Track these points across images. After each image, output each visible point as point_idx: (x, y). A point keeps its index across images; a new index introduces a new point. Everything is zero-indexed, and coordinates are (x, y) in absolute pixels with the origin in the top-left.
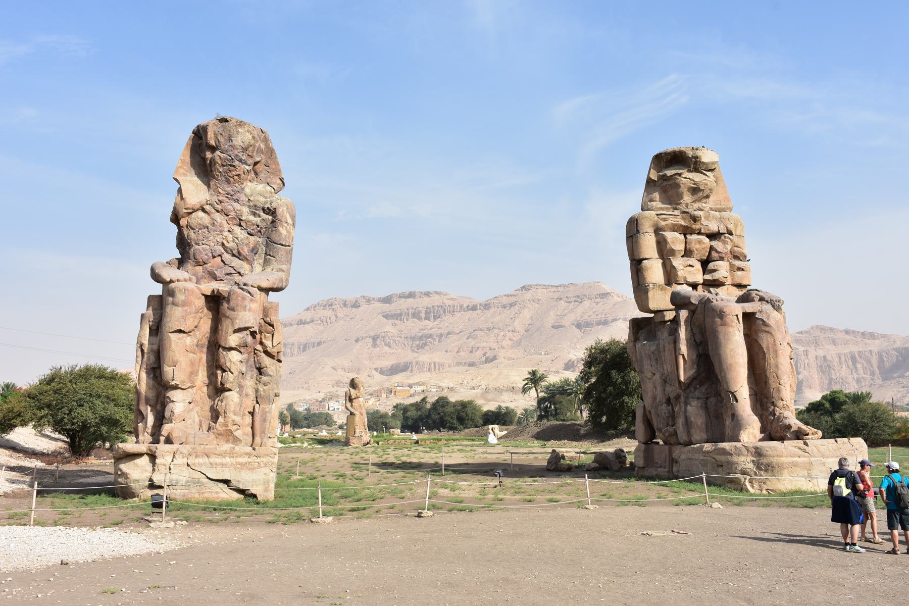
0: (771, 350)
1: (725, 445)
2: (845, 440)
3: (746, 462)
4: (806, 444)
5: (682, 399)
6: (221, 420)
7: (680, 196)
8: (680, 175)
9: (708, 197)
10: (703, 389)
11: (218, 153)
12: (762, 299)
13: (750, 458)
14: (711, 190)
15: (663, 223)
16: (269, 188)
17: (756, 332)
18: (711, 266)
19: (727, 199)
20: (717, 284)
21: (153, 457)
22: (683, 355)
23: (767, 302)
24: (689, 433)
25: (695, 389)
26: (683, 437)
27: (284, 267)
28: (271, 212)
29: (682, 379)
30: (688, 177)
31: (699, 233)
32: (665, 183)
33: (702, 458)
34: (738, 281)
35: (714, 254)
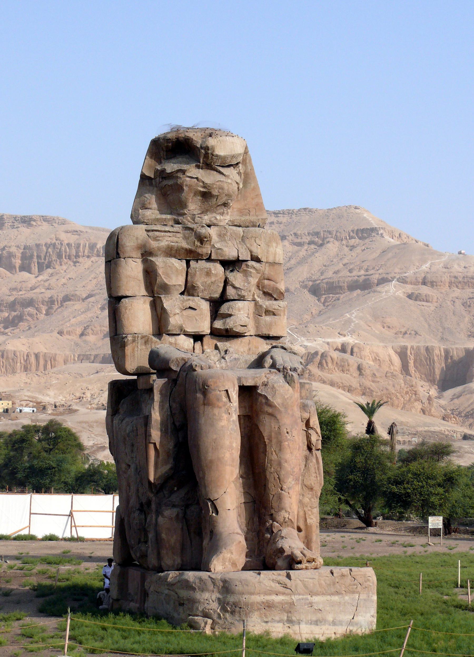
0: (274, 441)
1: (191, 575)
2: (345, 570)
3: (209, 599)
4: (289, 576)
5: (153, 506)
7: (183, 205)
8: (183, 172)
9: (225, 205)
10: (182, 492)
12: (273, 366)
13: (216, 595)
14: (229, 196)
15: (154, 244)
17: (257, 415)
18: (224, 309)
19: (259, 206)
20: (229, 335)
22: (155, 444)
23: (279, 370)
24: (159, 557)
25: (172, 492)
26: (152, 560)
29: (152, 478)
30: (194, 174)
31: (209, 259)
32: (165, 182)
33: (166, 592)
34: (265, 332)
35: (231, 292)
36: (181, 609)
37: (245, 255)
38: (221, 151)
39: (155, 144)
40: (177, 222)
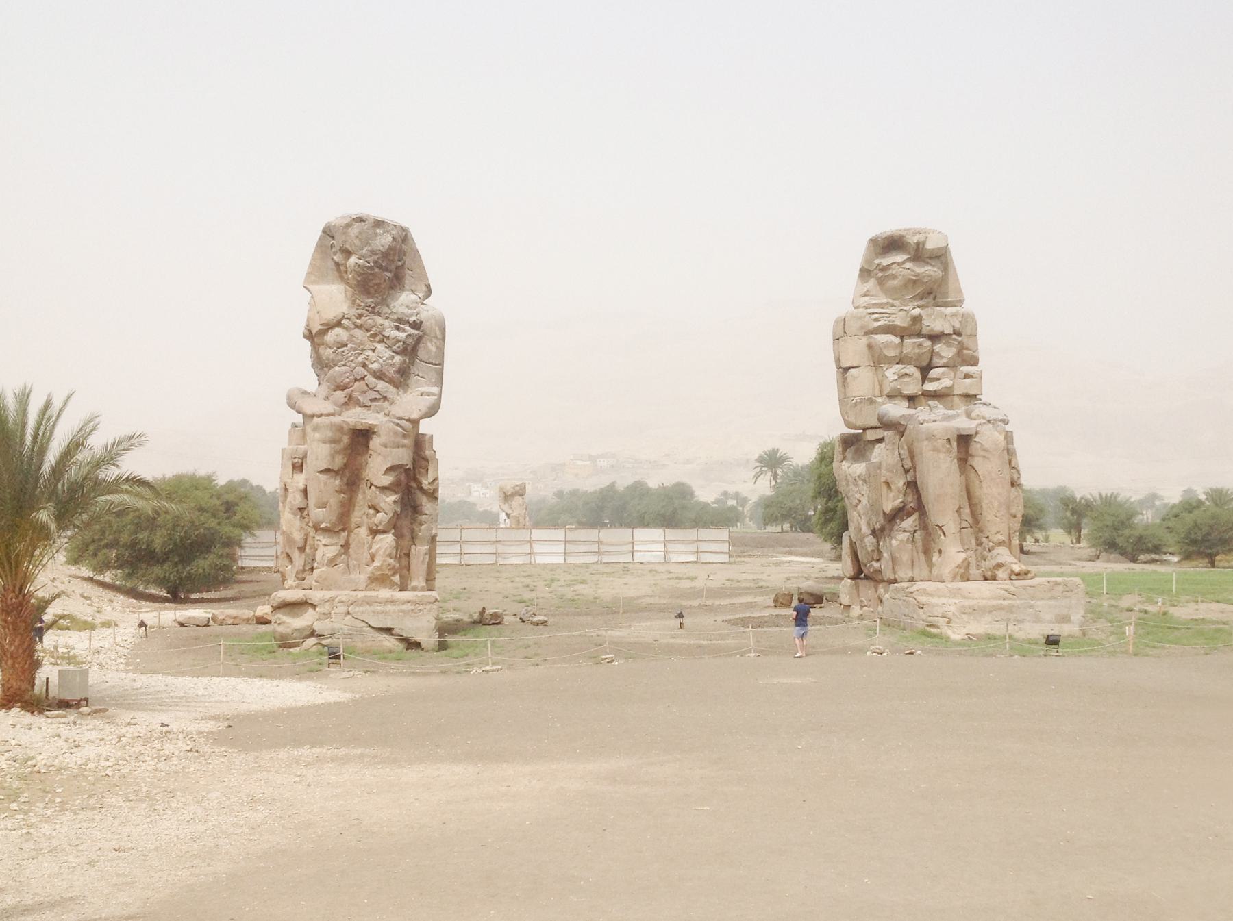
6: (377, 563)
8: (899, 264)
11: (353, 260)
16: (413, 297)
18: (933, 373)
21: (314, 606)
27: (435, 390)
28: (416, 325)
31: (919, 335)
36: (921, 611)
37: (948, 330)
38: (930, 245)
39: (873, 241)
40: (893, 306)
